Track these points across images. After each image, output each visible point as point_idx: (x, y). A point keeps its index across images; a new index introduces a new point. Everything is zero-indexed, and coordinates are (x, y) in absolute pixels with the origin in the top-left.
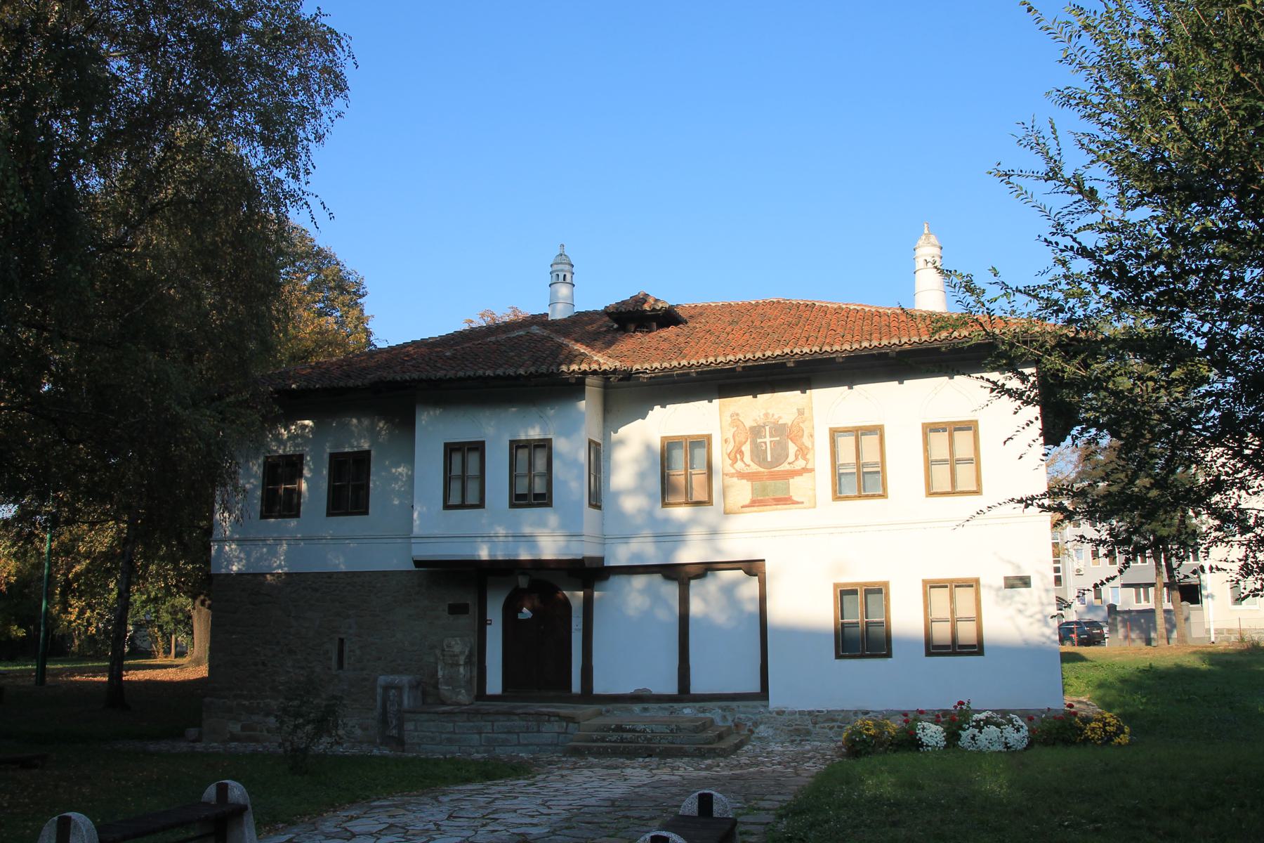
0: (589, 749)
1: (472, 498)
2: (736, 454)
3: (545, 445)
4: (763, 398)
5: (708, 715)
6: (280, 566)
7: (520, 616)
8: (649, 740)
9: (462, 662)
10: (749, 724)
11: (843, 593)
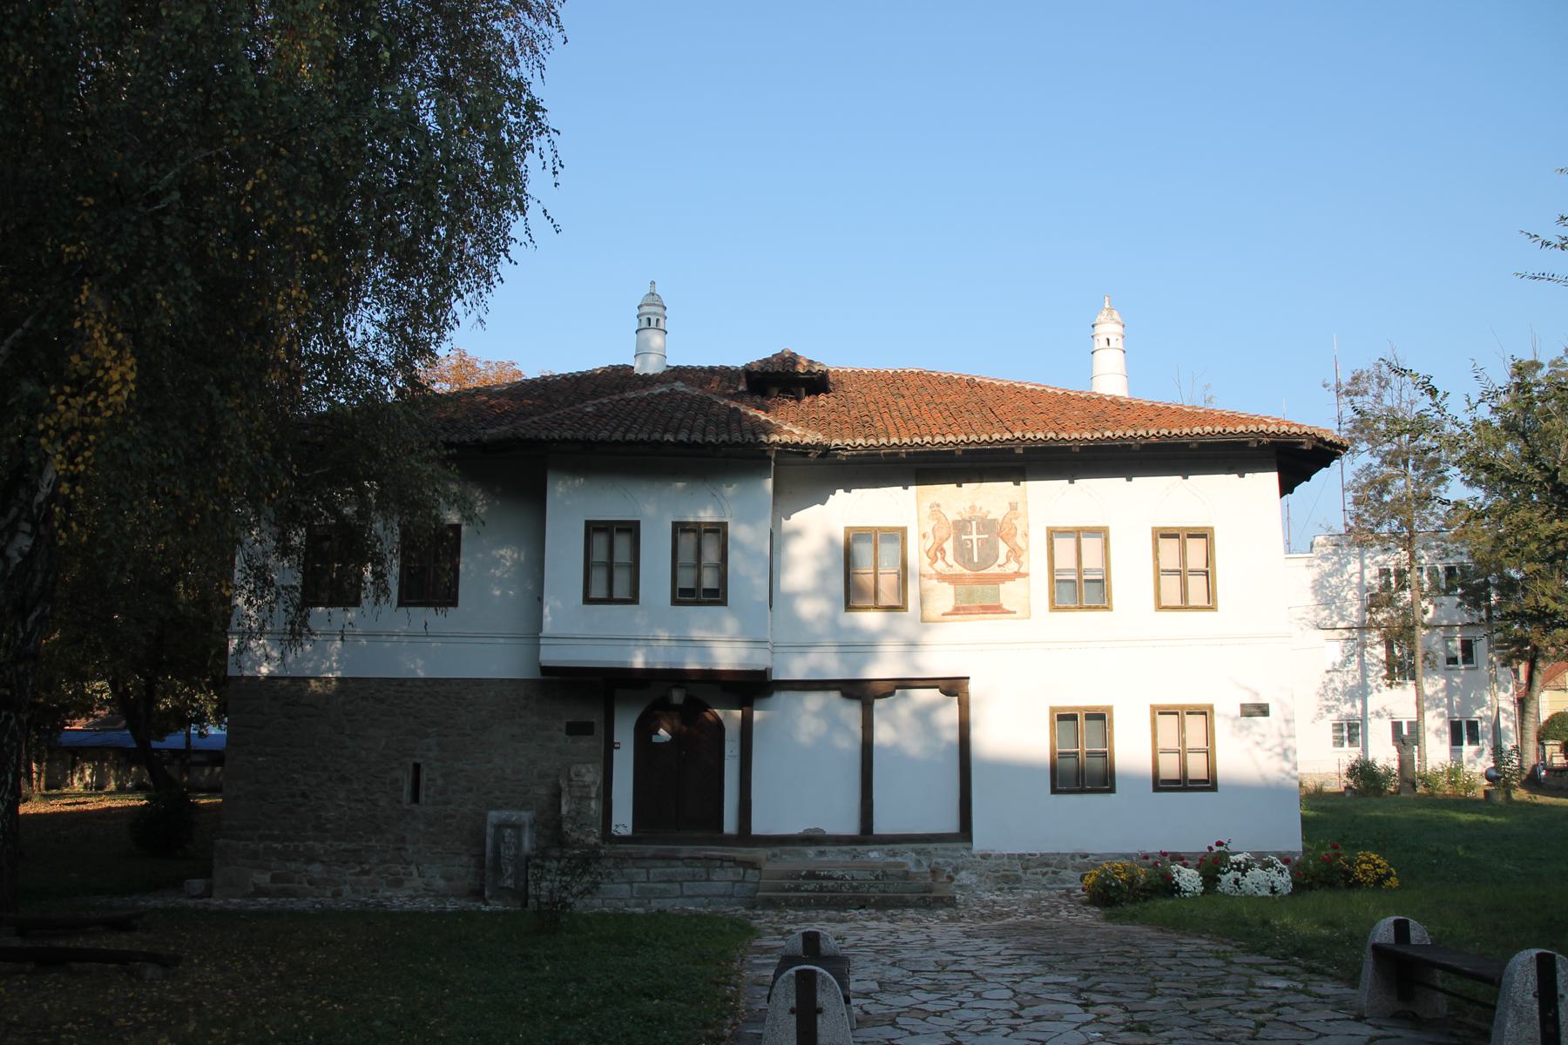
0: (787, 900)
1: (621, 590)
2: (937, 552)
3: (719, 530)
4: (969, 488)
5: (899, 859)
6: (330, 669)
7: (655, 739)
8: (855, 889)
10: (949, 869)
11: (1061, 718)
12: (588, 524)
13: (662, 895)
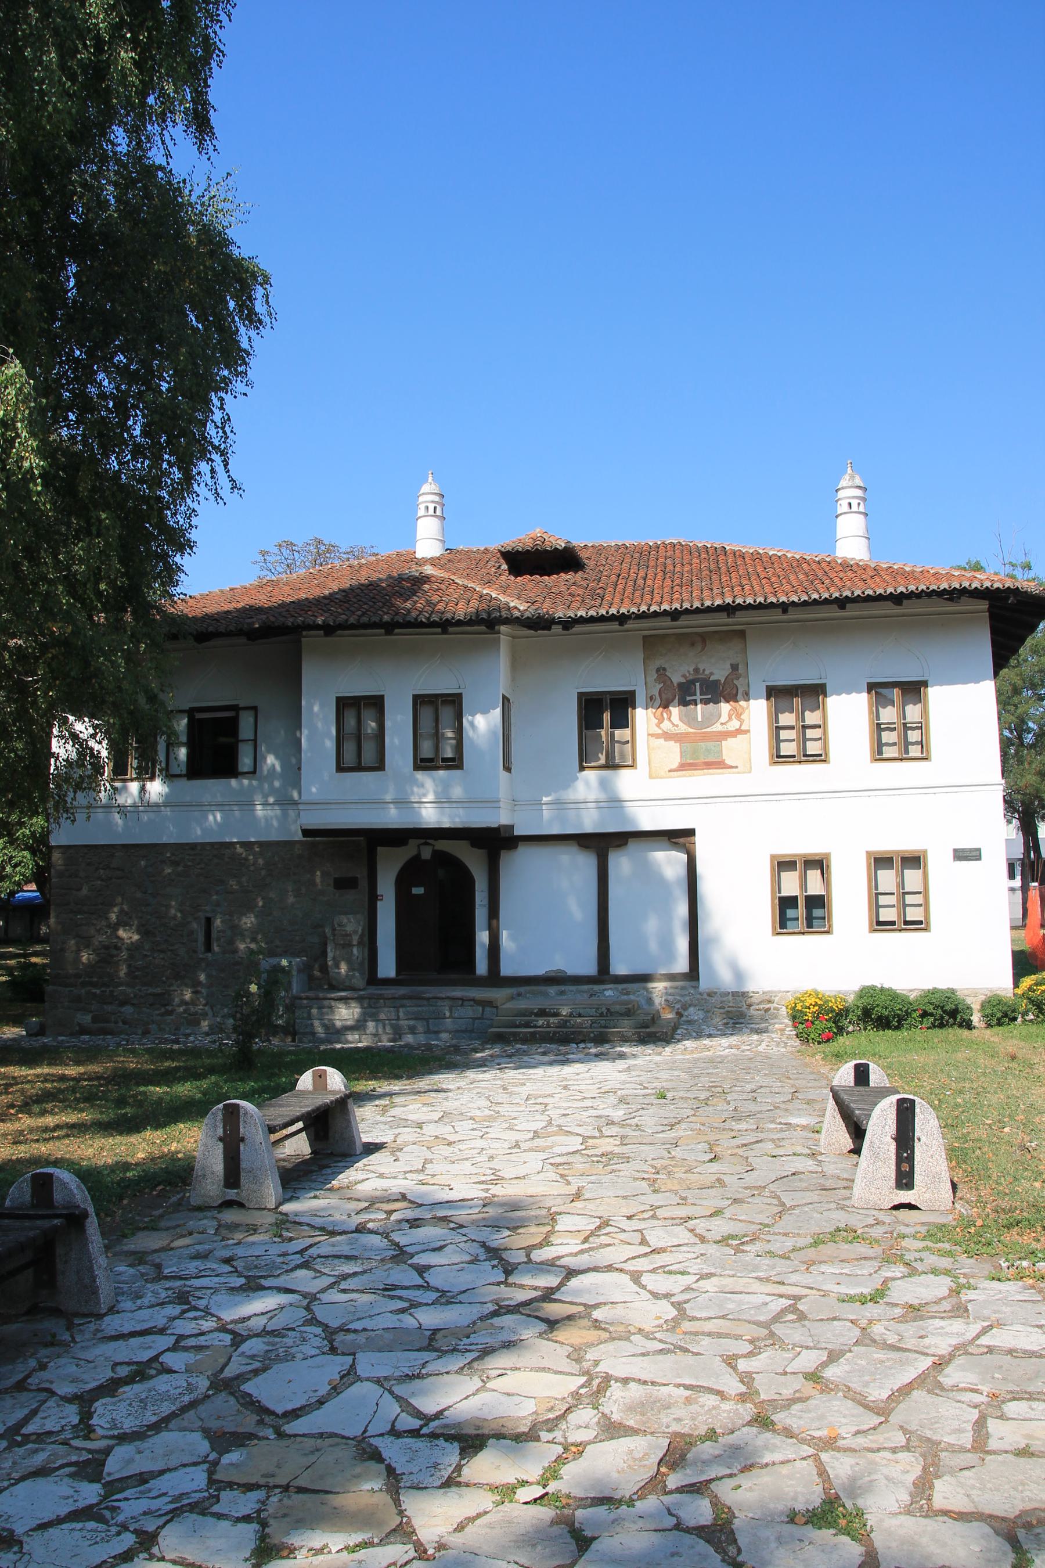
0: (514, 1034)
5: (632, 997)
9: (355, 942)
12: (339, 700)
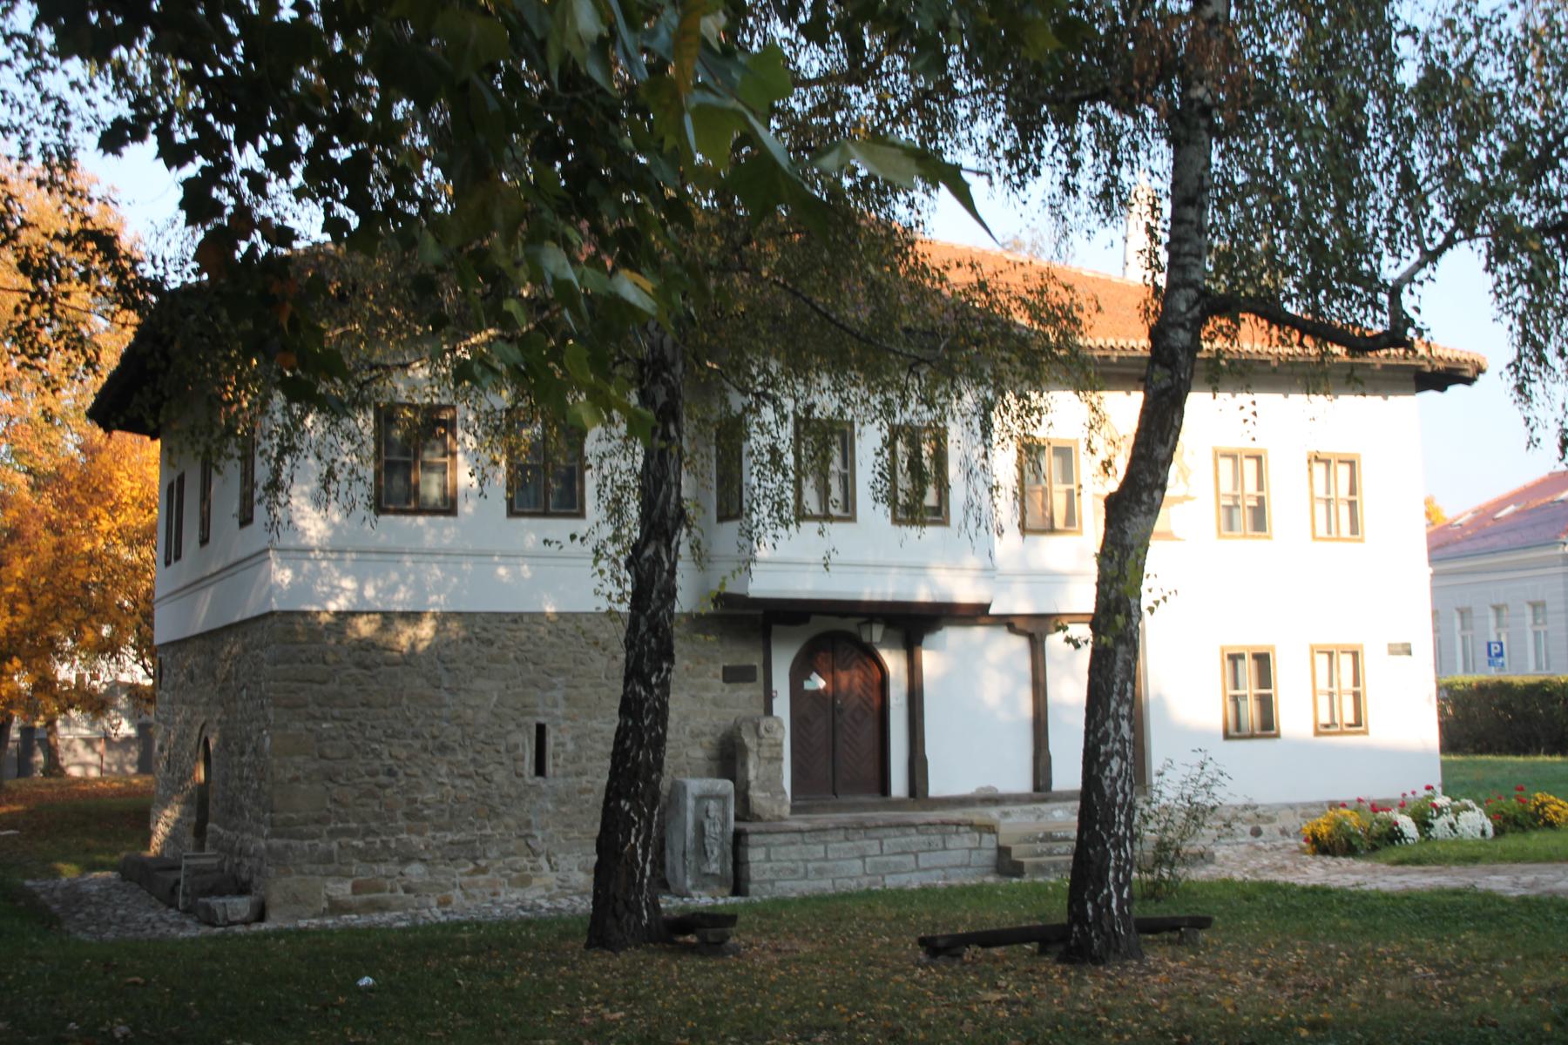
13: (896, 872)
